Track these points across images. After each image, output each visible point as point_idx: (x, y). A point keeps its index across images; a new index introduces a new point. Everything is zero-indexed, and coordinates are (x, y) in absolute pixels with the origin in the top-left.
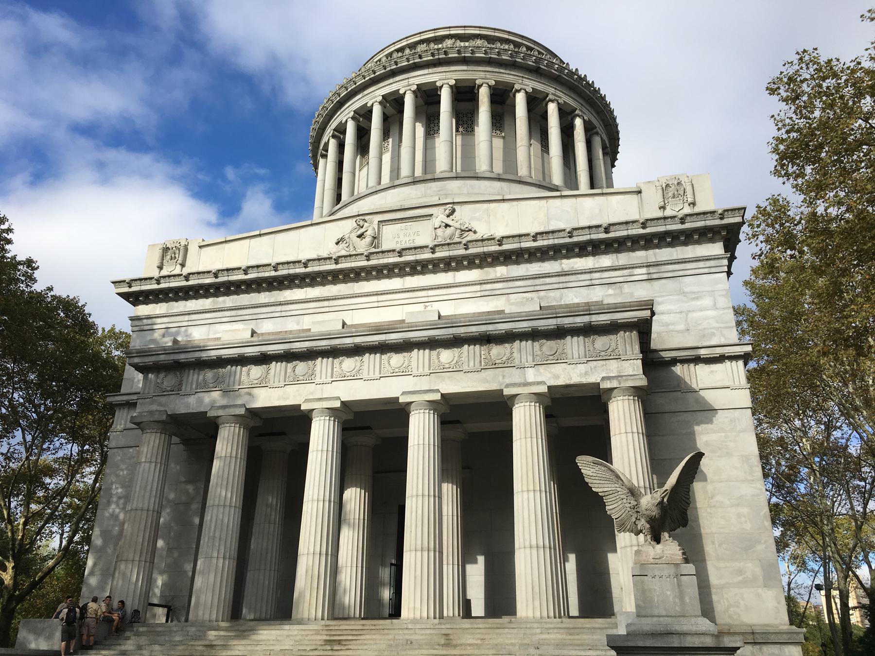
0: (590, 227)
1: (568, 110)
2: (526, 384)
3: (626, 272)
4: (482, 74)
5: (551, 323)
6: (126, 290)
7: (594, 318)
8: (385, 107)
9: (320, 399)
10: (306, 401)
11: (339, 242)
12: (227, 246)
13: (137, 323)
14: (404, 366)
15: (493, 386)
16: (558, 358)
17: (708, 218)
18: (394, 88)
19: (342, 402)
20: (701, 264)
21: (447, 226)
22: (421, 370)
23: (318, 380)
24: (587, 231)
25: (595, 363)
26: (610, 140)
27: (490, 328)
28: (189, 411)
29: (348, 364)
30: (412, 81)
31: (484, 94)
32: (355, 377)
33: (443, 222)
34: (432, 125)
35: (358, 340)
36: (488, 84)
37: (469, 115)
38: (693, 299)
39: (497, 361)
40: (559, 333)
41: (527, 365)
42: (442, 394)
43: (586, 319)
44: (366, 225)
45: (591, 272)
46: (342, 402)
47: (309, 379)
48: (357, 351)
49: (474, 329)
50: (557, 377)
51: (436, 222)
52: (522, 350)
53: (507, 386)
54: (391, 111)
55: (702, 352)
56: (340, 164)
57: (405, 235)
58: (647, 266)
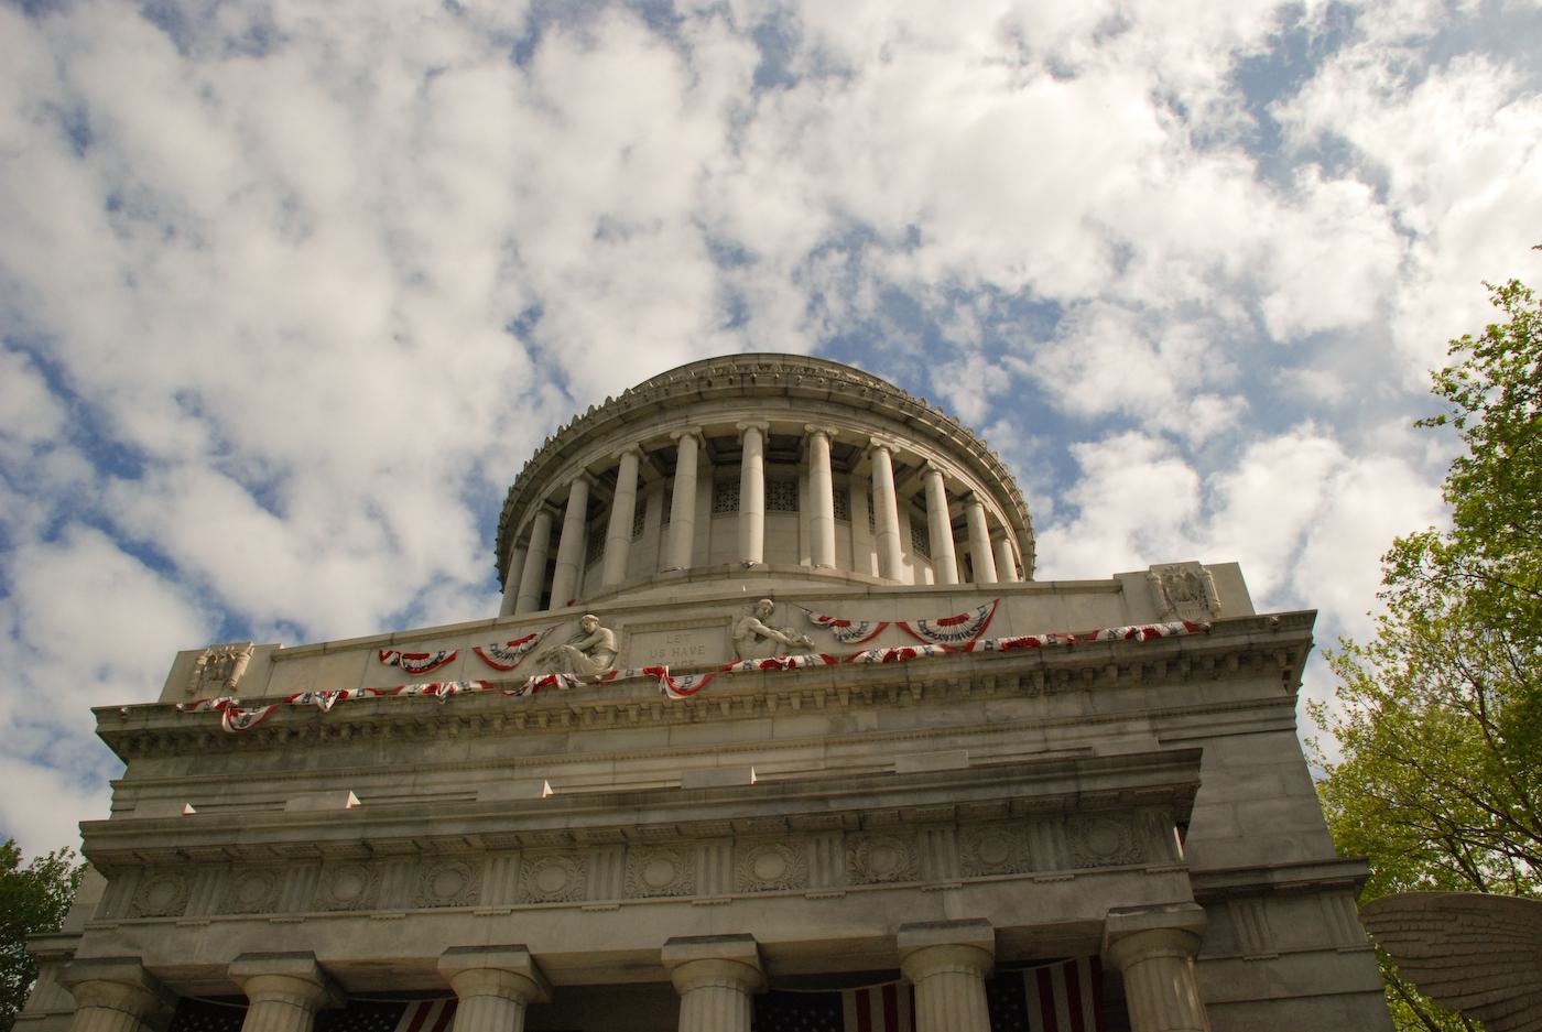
1: (958, 492)
4: (816, 418)
6: (113, 727)
7: (1085, 786)
8: (641, 462)
10: (452, 950)
11: (543, 659)
12: (325, 660)
13: (124, 794)
14: (674, 883)
15: (875, 931)
17: (1253, 631)
18: (661, 429)
19: (534, 960)
20: (1248, 715)
21: (760, 637)
22: (713, 890)
23: (484, 908)
25: (1093, 880)
26: (1023, 555)
27: (867, 804)
28: (189, 962)
33: (750, 630)
34: (722, 498)
36: (826, 433)
37: (789, 486)
38: (1244, 778)
39: (881, 877)
40: (1015, 818)
41: (946, 883)
42: (758, 945)
43: (1070, 787)
45: (1044, 727)
49: (834, 806)
53: (905, 927)
54: (653, 473)
55: (1277, 877)
56: (550, 567)
58: (1152, 717)
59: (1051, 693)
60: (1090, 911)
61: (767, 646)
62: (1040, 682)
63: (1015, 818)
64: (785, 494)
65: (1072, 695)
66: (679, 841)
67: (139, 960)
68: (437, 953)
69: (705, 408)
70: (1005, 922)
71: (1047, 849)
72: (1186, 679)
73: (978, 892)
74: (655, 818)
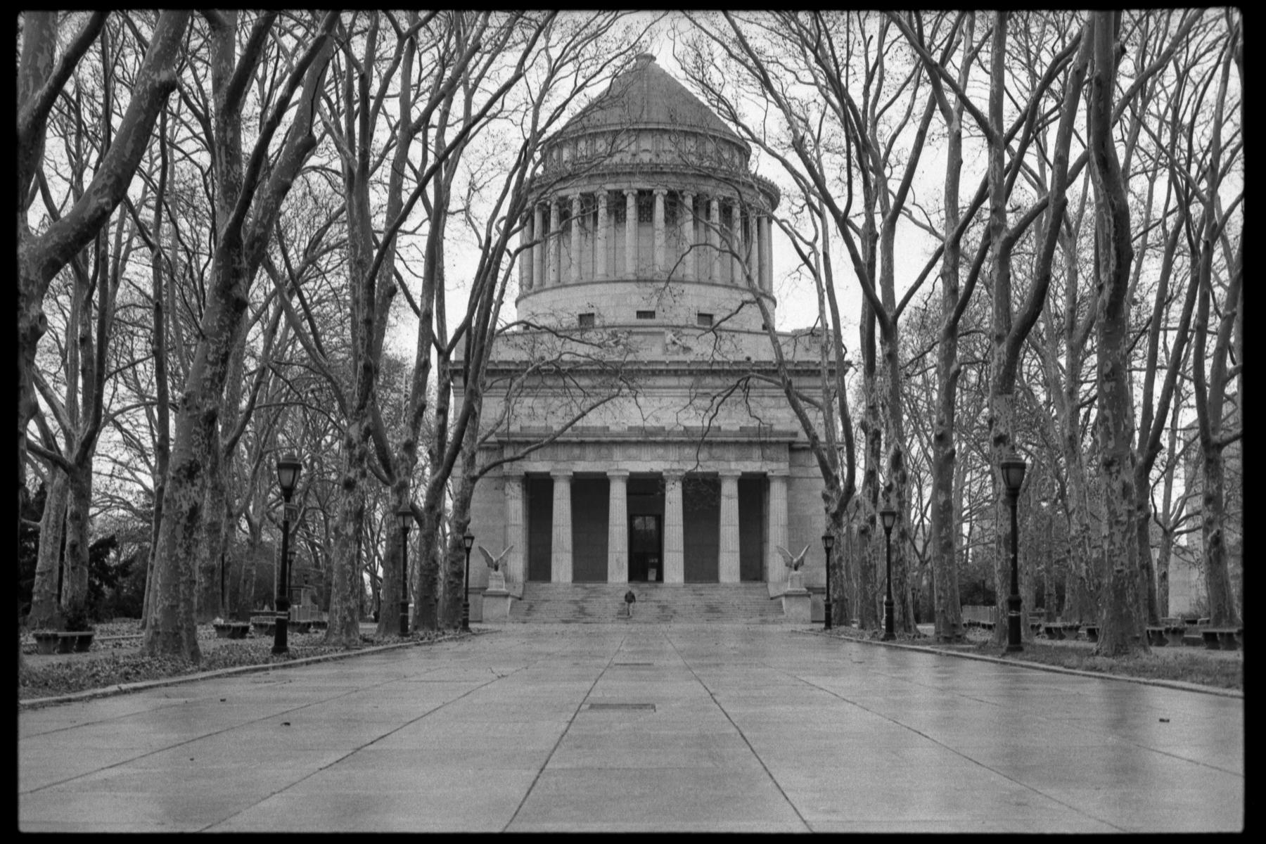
2: (730, 470)
5: (746, 439)
16: (749, 458)
21: (674, 343)
29: (633, 451)
30: (633, 185)
40: (750, 444)
47: (609, 458)
50: (746, 467)
51: (668, 341)
52: (731, 453)
60: (764, 470)
61: (675, 348)
63: (750, 444)
64: (672, 216)
66: (665, 444)
71: (757, 452)
72: (809, 376)
74: (659, 439)
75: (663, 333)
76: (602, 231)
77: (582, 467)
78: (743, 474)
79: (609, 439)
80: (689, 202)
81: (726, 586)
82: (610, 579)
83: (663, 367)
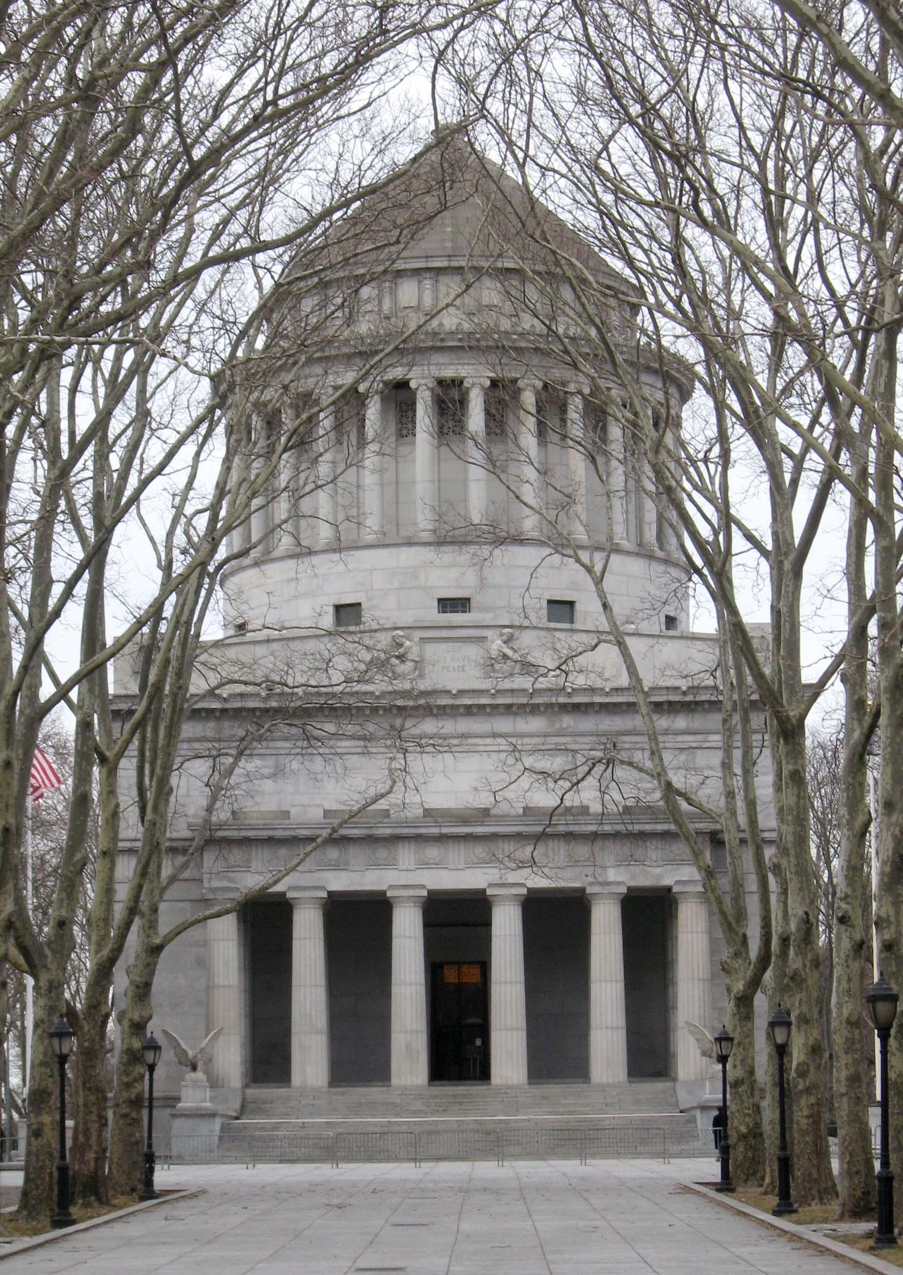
0: (668, 688)
2: (609, 884)
3: (699, 737)
9: (405, 887)
10: (391, 887)
15: (577, 884)
19: (429, 891)
21: (505, 657)
24: (665, 692)
29: (432, 852)
31: (529, 399)
32: (437, 865)
35: (444, 830)
41: (608, 864)
44: (408, 643)
46: (429, 891)
47: (392, 864)
48: (442, 839)
51: (494, 654)
52: (609, 854)
53: (591, 884)
57: (453, 659)
59: (669, 712)
60: (667, 882)
62: (666, 707)
65: (681, 715)
67: (238, 889)
68: (385, 888)
69: (437, 358)
70: (633, 884)
73: (622, 869)
75: (483, 639)
76: (370, 459)
77: (340, 882)
78: (630, 889)
79: (388, 831)
80: (529, 399)
81: (603, 1088)
82: (395, 1081)
83: (484, 701)
